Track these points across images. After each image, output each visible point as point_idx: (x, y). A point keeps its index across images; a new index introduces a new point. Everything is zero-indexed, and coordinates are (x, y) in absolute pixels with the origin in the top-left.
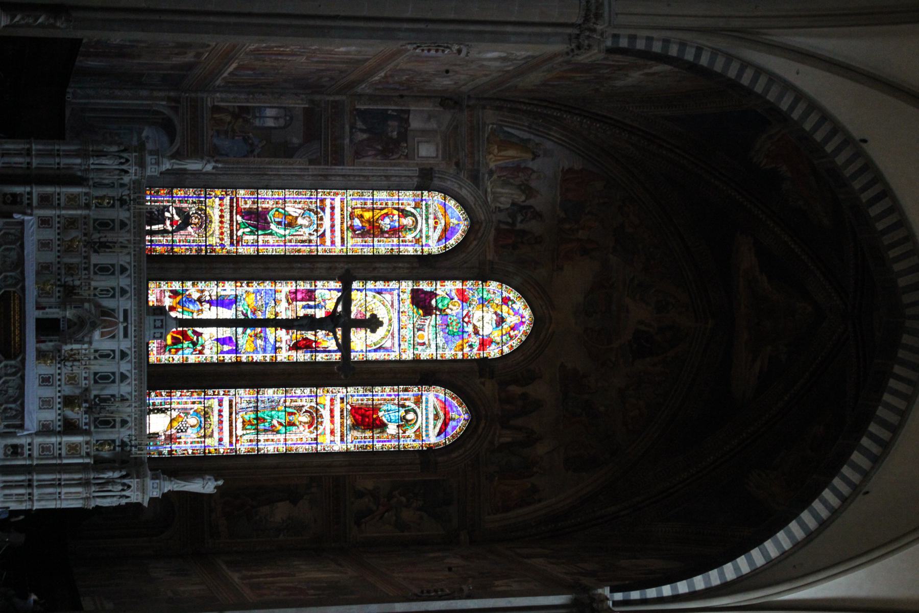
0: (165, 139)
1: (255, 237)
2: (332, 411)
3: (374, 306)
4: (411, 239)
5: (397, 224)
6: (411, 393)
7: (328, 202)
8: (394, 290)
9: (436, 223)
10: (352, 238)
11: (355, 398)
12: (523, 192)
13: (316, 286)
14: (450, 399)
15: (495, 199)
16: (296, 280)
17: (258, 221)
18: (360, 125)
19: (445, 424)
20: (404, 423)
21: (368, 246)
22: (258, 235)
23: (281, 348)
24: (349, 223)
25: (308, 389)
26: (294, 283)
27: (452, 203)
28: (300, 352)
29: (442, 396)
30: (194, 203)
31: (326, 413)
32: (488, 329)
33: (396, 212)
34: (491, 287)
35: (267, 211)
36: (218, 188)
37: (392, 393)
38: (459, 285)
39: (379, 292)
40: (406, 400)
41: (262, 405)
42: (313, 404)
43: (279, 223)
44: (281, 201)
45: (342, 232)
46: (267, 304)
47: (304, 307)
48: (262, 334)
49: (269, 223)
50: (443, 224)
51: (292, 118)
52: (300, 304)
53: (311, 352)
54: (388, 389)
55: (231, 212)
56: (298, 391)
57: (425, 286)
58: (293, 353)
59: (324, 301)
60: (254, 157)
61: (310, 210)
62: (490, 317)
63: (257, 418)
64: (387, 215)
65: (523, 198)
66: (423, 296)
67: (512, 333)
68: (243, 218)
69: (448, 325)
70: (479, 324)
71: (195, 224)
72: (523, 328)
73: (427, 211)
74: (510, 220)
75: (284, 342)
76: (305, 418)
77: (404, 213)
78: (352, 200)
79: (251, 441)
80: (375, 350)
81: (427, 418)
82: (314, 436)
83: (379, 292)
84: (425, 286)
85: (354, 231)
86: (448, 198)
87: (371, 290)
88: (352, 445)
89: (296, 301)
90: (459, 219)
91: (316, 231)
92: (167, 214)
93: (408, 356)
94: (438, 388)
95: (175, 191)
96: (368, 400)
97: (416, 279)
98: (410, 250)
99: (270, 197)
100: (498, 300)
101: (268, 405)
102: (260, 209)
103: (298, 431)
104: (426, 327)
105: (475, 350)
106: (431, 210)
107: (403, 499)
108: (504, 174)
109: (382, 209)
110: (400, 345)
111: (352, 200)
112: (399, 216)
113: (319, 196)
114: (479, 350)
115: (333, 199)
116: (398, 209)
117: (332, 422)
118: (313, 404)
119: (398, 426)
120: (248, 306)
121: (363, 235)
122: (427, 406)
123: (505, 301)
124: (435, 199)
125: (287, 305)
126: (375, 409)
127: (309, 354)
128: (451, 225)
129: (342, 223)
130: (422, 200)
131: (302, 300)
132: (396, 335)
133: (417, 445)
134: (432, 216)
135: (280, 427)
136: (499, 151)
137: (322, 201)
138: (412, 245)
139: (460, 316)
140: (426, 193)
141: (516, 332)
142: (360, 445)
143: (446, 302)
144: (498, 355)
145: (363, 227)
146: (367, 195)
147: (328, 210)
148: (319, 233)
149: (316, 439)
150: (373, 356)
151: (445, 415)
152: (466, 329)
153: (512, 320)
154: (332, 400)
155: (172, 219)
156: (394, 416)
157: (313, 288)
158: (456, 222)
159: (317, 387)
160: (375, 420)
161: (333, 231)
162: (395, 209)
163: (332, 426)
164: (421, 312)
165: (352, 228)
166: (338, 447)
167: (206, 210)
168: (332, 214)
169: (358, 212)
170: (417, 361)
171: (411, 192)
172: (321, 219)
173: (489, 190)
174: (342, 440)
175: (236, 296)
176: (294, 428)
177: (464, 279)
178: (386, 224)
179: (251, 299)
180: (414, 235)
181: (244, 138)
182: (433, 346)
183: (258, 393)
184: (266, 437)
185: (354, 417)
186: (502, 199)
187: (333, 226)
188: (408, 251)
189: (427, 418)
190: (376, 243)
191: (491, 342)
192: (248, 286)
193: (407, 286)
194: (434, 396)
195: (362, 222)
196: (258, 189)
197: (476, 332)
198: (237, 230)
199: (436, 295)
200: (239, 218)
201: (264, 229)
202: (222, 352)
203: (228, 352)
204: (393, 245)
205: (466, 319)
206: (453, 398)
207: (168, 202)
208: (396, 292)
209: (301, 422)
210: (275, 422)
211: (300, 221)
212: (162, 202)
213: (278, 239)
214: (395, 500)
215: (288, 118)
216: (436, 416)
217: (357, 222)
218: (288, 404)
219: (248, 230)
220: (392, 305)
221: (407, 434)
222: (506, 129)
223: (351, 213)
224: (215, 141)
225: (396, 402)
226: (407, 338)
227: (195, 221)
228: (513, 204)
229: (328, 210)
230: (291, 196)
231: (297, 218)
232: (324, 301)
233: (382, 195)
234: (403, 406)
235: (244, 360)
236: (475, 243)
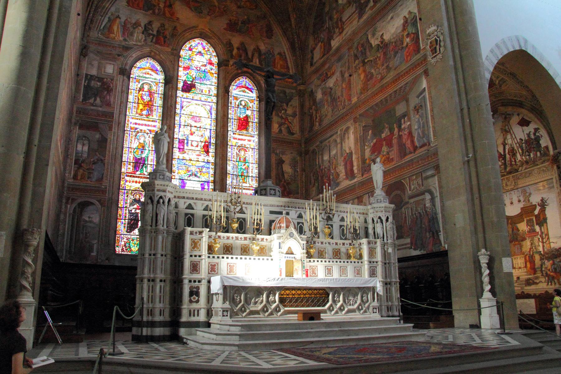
0: (91, 207)
1: (149, 165)
2: (239, 139)
3: (189, 111)
4: (156, 87)
5: (147, 93)
6: (233, 101)
7: (133, 126)
8: (181, 100)
9: (148, 74)
10: (153, 116)
11: (233, 127)
12: (137, 27)
13: (177, 138)
14: (236, 84)
15: (140, 41)
16: (173, 148)
17: (140, 163)
18: (92, 101)
19: (247, 88)
20: (246, 107)
21: (157, 109)
22: (148, 164)
23: (207, 160)
24: (145, 116)
25: (228, 149)
26: (174, 149)
27: (138, 64)
28: (210, 151)
29: (235, 87)
30: (127, 196)
31: (240, 143)
32: (204, 59)
33: (141, 92)
34: (183, 54)
35: (135, 158)
36: (120, 182)
37: (232, 110)
38: (181, 69)
39: (182, 107)
40: (235, 104)
41: (235, 172)
42: (236, 147)
43: (142, 152)
44: (130, 150)
45: (149, 121)
46: (184, 164)
47: (187, 146)
48: (200, 168)
49: (142, 158)
50: (149, 70)
51: (85, 137)
52: (186, 147)
53: (210, 145)
54: (230, 111)
55: (134, 177)
56: (229, 154)
57: (180, 85)
58: (210, 154)
59: (185, 135)
60: (105, 159)
61: (136, 136)
62: (198, 58)
63: (242, 176)
64: (142, 97)
65: (140, 28)
66: (185, 87)
67: (206, 49)
68: (137, 171)
69: (201, 78)
70: (201, 64)
71: (140, 197)
72: (205, 45)
73: (141, 77)
74: (152, 36)
75: (205, 158)
76: (242, 153)
77: (142, 89)
78: (132, 113)
79: (252, 180)
80: (211, 114)
81: (244, 96)
82: (251, 150)
83: (182, 107)
84: (180, 85)
85: (149, 115)
86: (135, 65)
87: (181, 111)
88: (256, 132)
89: (184, 149)
90: (147, 62)
91: (148, 134)
92: (133, 211)
93: (215, 99)
94: (231, 88)
95: (120, 206)
96: (235, 121)
97: (177, 89)
98: (161, 89)
99: (127, 155)
100: (190, 52)
101: (235, 170)
102: (134, 161)
103: (248, 157)
104: (201, 88)
105: (214, 68)
106: (141, 75)
107: (283, 112)
108: (126, 33)
109: (139, 99)
110: (209, 102)
111: (132, 113)
112: (143, 91)
113: (129, 130)
114: (213, 66)
115: (131, 123)
116: (139, 91)
117: (245, 140)
118: (236, 147)
119: (248, 110)
120: (185, 173)
121: (152, 111)
122: (239, 95)
123: (190, 49)
124: (135, 72)
125: (186, 154)
126: (240, 119)
127: (211, 146)
128: (150, 67)
129: (144, 120)
130: (135, 78)
131: (184, 146)
132: (204, 103)
133: (256, 103)
134: (145, 75)
135: (246, 166)
136: (114, 33)
137: (131, 128)
138: (159, 87)
139: (197, 71)
140: (131, 76)
141: (206, 47)
142: (255, 129)
143: (189, 77)
144: (217, 58)
145: (147, 110)
146: (130, 105)
147: (137, 126)
148: (149, 132)
149: (252, 149)
150: (214, 116)
151: (243, 87)
152: (203, 70)
153: (200, 48)
154: (234, 138)
155: (136, 209)
156: (243, 111)
157: (177, 139)
158: (148, 64)
159: (227, 145)
160: (244, 119)
161: (149, 126)
162: (139, 92)
163: (247, 140)
164: (193, 89)
165: (147, 116)
166: (256, 139)
167: (132, 190)
168: (139, 124)
169: (139, 111)
170: (217, 96)
171: (131, 83)
172: (141, 130)
173: (134, 43)
174: (253, 137)
175: (180, 179)
176: (247, 159)
177: (179, 66)
178: (147, 98)
179: (182, 172)
180: (154, 86)
181: (94, 164)
182: (211, 87)
183: (229, 174)
184: (250, 172)
185: (242, 129)
186: (140, 38)
187: (146, 125)
188: (162, 90)
189: (244, 96)
190: (156, 105)
191: (210, 60)
192: (175, 172)
193: (180, 93)
194: (234, 91)
195: (144, 110)
196: (122, 161)
197: (205, 66)
198: (144, 175)
199: (185, 80)
200: (138, 173)
201: (144, 161)
202: (208, 189)
203: (209, 186)
204: (158, 97)
205: (198, 69)
206: (236, 82)
207: (126, 210)
208: (183, 100)
209: (244, 155)
210: (244, 167)
211: (142, 141)
212: (126, 214)
213: (150, 154)
214: (283, 115)
215: (84, 138)
216: (244, 91)
217: (145, 112)
218: (235, 160)
219: (144, 169)
220: (189, 102)
221: (251, 106)
222: (102, 28)
223: (139, 115)
224: (94, 180)
225: (236, 109)
226: (206, 98)
227: (138, 197)
228: (143, 33)
229: (137, 126)
230: (128, 144)
231: (140, 143)
232: (185, 135)
233: (131, 98)
234: (238, 106)
235: (213, 179)
236: (161, 55)
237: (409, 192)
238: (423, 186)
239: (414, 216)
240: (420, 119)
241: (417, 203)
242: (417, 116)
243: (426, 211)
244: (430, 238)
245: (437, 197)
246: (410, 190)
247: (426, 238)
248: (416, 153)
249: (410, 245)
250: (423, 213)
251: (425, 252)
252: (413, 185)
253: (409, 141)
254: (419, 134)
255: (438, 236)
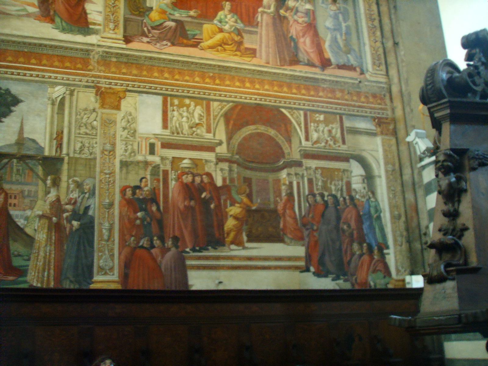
237: (304, 142)
238: (344, 142)
239: (318, 198)
240: (341, 17)
241: (328, 174)
242: (333, 8)
243: (352, 199)
244: (361, 256)
245: (380, 177)
246: (307, 139)
247: (353, 254)
248: (326, 72)
249: (302, 263)
250: (345, 199)
251: (347, 286)
252: (316, 131)
253: (308, 41)
254: (334, 40)
255: (383, 256)
